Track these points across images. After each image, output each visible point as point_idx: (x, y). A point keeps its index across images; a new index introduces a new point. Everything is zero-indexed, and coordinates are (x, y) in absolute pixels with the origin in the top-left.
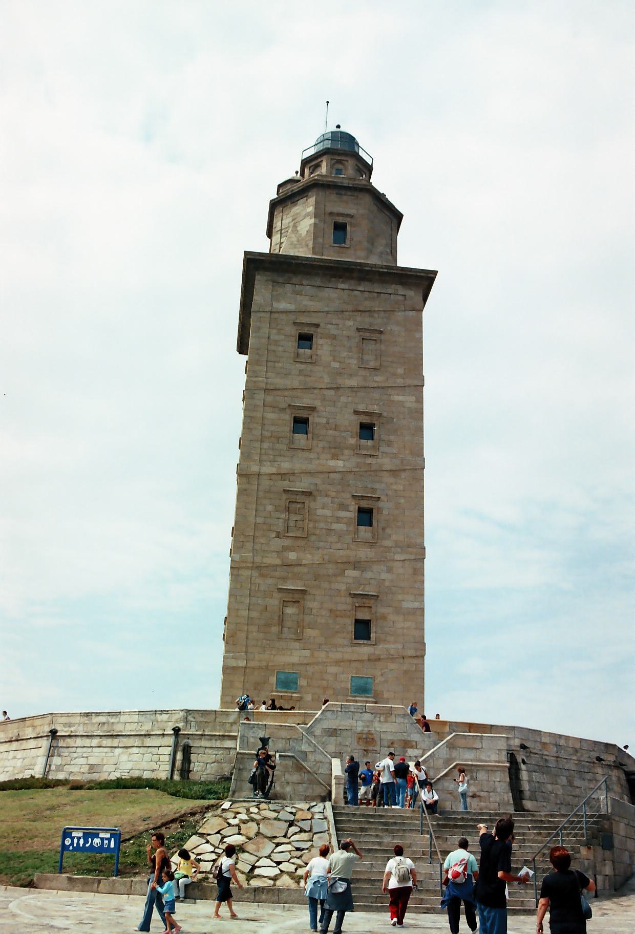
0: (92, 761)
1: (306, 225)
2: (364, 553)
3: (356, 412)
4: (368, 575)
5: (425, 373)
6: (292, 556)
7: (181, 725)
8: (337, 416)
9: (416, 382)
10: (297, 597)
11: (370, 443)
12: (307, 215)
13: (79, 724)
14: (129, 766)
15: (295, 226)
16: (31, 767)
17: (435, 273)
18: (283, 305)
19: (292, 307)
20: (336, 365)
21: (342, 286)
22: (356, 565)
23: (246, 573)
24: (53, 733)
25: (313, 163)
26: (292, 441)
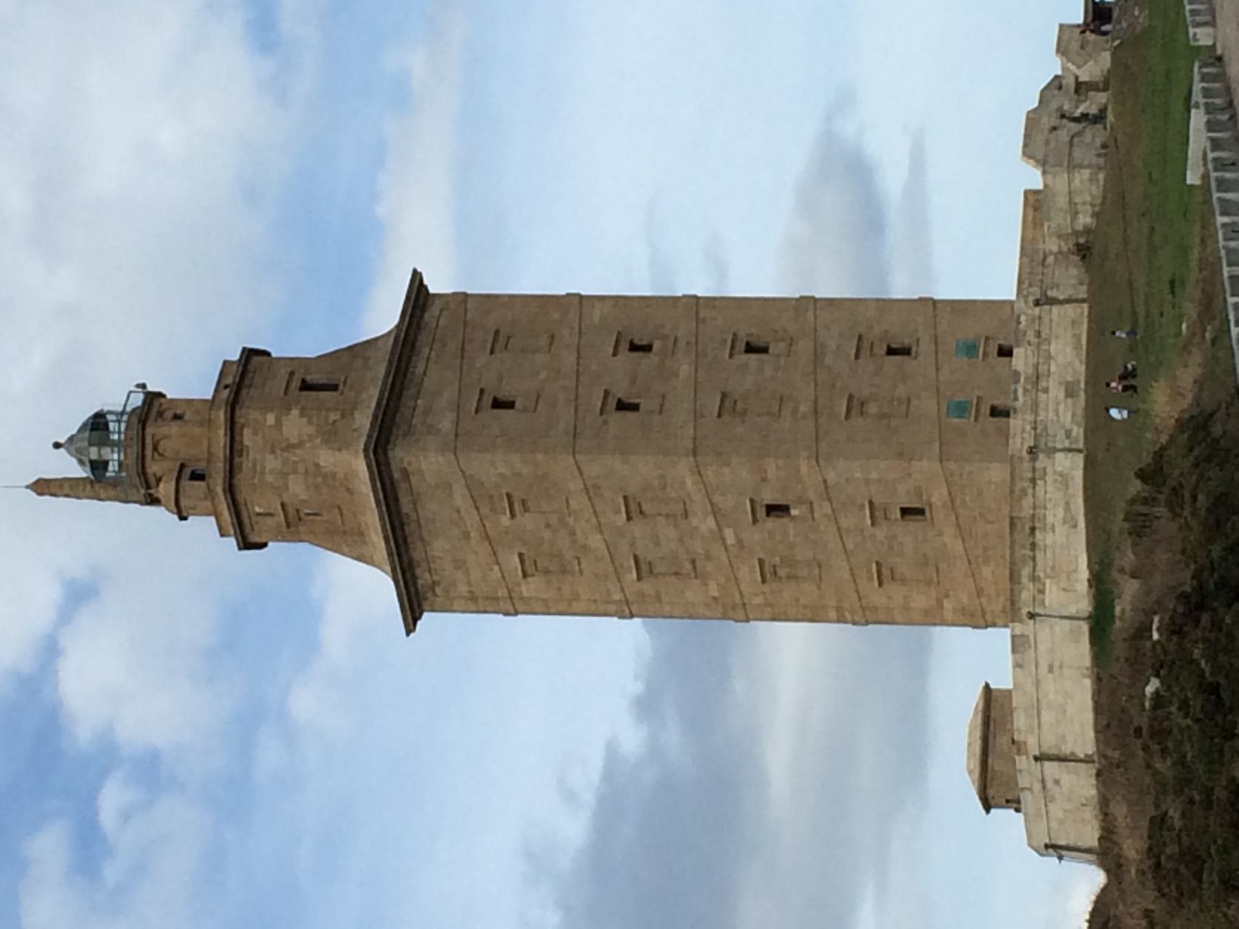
0: (1062, 395)
1: (295, 425)
2: (804, 347)
3: (615, 354)
4: (832, 345)
5: (561, 291)
6: (803, 408)
7: (1031, 299)
8: (620, 373)
9: (576, 301)
10: (856, 406)
11: (657, 345)
12: (279, 421)
13: (1024, 420)
14: (1069, 350)
15: (289, 447)
16: (1065, 479)
17: (415, 271)
18: (446, 424)
19: (451, 416)
20: (543, 376)
21: (420, 370)
22: (817, 358)
23: (824, 447)
24: (1031, 451)
25: (149, 451)
26: (650, 412)
